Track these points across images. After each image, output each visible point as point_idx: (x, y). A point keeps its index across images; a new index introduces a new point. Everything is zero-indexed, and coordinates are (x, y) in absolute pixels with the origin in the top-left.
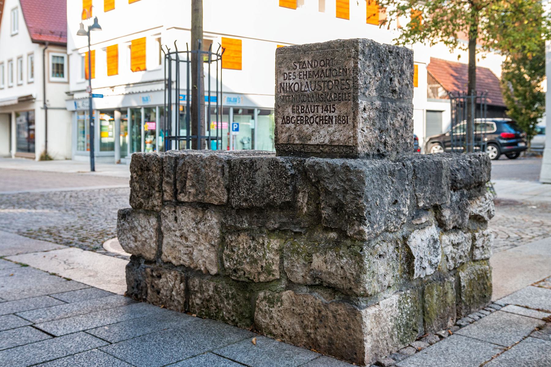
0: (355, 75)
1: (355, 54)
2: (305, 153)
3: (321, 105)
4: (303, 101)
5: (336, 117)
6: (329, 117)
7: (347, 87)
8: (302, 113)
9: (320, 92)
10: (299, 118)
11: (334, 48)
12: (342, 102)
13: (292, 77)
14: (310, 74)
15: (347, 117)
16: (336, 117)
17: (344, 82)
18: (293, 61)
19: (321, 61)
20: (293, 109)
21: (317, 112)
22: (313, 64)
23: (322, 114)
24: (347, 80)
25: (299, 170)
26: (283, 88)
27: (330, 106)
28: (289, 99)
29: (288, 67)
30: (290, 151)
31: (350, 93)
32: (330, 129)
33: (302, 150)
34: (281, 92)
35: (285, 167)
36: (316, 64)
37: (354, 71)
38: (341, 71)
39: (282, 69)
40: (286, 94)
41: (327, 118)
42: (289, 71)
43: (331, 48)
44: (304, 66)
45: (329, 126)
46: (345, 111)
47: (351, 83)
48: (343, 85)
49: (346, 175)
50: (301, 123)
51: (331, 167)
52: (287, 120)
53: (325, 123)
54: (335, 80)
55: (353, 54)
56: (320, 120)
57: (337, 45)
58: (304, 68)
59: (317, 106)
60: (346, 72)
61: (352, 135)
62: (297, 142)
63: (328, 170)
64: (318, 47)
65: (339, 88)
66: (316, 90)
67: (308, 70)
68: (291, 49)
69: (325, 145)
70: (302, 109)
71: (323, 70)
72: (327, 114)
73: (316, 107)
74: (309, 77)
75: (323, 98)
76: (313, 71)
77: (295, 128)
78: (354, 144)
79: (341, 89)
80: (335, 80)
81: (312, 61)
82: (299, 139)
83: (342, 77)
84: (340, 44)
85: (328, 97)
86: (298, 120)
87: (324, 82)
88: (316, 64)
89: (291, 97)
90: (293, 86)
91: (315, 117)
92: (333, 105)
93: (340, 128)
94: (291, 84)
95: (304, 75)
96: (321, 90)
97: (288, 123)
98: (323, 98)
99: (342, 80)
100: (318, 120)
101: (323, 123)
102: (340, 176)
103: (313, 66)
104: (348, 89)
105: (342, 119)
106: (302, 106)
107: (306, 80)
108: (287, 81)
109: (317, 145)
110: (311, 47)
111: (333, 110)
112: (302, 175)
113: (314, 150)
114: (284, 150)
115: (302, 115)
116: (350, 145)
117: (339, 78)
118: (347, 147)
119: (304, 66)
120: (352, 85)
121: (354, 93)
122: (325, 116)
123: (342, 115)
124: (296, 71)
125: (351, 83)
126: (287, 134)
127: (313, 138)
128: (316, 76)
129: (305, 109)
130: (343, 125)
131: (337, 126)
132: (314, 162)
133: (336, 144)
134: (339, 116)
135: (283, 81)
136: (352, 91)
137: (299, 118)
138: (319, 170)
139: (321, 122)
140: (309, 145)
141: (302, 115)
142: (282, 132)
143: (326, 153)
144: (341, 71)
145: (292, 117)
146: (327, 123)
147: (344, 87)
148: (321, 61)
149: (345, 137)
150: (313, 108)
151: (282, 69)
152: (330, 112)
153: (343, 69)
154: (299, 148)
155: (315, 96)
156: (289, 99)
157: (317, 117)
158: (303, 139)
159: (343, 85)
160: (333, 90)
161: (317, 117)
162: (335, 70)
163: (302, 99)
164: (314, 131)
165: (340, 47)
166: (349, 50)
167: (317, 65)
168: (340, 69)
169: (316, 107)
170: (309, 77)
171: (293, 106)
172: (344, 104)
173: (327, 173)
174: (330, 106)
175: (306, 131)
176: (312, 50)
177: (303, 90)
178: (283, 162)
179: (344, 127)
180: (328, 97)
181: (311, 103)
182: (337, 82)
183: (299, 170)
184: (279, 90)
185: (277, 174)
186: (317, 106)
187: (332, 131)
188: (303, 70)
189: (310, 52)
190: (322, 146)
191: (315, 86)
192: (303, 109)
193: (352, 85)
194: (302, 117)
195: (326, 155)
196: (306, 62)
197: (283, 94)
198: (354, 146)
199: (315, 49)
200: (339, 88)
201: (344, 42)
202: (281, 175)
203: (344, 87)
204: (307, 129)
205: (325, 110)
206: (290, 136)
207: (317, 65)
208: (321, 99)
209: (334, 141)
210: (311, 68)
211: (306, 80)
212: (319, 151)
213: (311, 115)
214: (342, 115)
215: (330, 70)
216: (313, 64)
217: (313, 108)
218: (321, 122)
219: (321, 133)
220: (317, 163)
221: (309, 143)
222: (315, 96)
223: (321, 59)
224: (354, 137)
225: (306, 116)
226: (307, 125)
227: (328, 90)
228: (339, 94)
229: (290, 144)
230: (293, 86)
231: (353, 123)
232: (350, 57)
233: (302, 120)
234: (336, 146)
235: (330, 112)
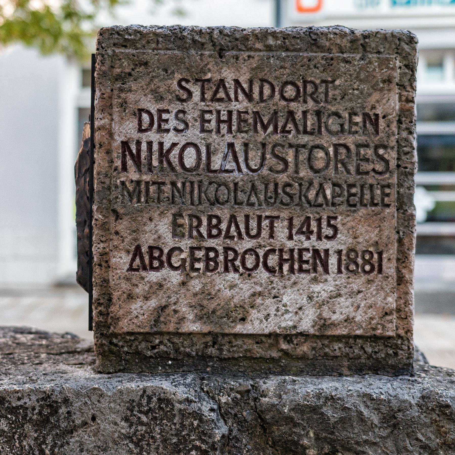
0: (404, 134)
1: (403, 75)
2: (221, 360)
3: (285, 214)
4: (217, 201)
5: (339, 252)
6: (316, 252)
7: (379, 167)
8: (210, 236)
9: (283, 178)
10: (200, 254)
11: (329, 50)
12: (363, 211)
13: (173, 123)
14: (239, 120)
15: (380, 254)
16: (339, 252)
17: (370, 152)
18: (178, 76)
19: (286, 83)
20: (175, 225)
21: (271, 236)
22: (256, 90)
23: (290, 244)
24: (376, 148)
25: (241, 422)
26: (137, 159)
27: (319, 221)
28: (160, 191)
29: (154, 91)
30: (165, 356)
31: (389, 186)
32: (317, 288)
33: (212, 351)
34: (125, 168)
35: (198, 416)
36: (267, 91)
37: (400, 122)
38: (358, 119)
39: (131, 97)
40: (146, 178)
41: (307, 256)
42: (161, 106)
43: (321, 48)
44: (221, 94)
45: (315, 280)
46: (373, 236)
47: (392, 156)
48: (367, 160)
49: (439, 433)
50: (207, 268)
51: (384, 409)
52: (152, 258)
53: (301, 270)
54: (336, 146)
55: (397, 74)
56: (281, 261)
57: (345, 43)
58: (221, 100)
59: (272, 219)
60: (376, 124)
61: (394, 306)
62: (195, 327)
63: (376, 419)
64: (271, 41)
65: (352, 169)
66: (265, 171)
67: (235, 106)
68: (165, 36)
69: (301, 334)
70: (210, 227)
71: (291, 114)
72: (306, 244)
73: (265, 223)
74: (240, 130)
75: (291, 196)
76: (256, 114)
77: (183, 284)
78: (401, 332)
79: (358, 172)
80: (336, 146)
81: (251, 82)
82: (199, 318)
83: (361, 138)
84: (352, 42)
85: (312, 194)
86: (195, 260)
87: (297, 148)
88: (267, 91)
89: (167, 188)
90: (176, 152)
91: (261, 253)
92: (329, 218)
93: (355, 287)
94: (167, 146)
95: (219, 121)
96: (285, 170)
97: (157, 269)
98: (291, 196)
99: (359, 146)
100: (273, 261)
101: (292, 270)
102: (420, 436)
103: (256, 95)
104: (380, 173)
105: (360, 261)
106: (210, 218)
107: (229, 138)
108: (153, 136)
109: (269, 336)
110: (246, 38)
111: (330, 232)
112: (252, 435)
113: (258, 351)
114: (138, 353)
115: (211, 243)
116: (390, 333)
117: (350, 140)
118: (375, 339)
119: (221, 94)
120: (393, 164)
121: (400, 185)
122: (301, 251)
123: (360, 248)
124: (188, 106)
125: (392, 156)
126: (153, 303)
127: (254, 314)
128: (265, 128)
129: (224, 226)
130: (364, 278)
131: (342, 279)
132: (318, 396)
133: (342, 331)
134: (351, 250)
135: (136, 135)
136: (394, 180)
137: (200, 254)
138: (342, 420)
139: (286, 267)
140: (236, 336)
141: (211, 243)
142: (131, 297)
143: (303, 358)
144: (358, 119)
145: (172, 250)
146: (307, 271)
147: (368, 167)
148: (286, 83)
149: (371, 312)
150: (253, 224)
151: (131, 97)
152: (319, 238)
153: (366, 116)
154: (199, 346)
155: (261, 187)
156: (160, 191)
157: (273, 251)
158: (214, 318)
159: (367, 160)
160: (331, 172)
161: (273, 251)
162: (337, 114)
163: (212, 195)
164: (260, 294)
165: (353, 50)
166: (384, 63)
167: (272, 96)
168: (353, 113)
169: (265, 223)
170: (240, 130)
171: (179, 215)
172: (368, 217)
173: (372, 426)
174: (319, 221)
175: (228, 293)
176: (251, 49)
177: (216, 165)
178: (188, 401)
179: (369, 282)
180: (312, 194)
181: (247, 210)
182: (343, 151)
183: (241, 422)
184: (118, 163)
185: (165, 440)
186: (272, 219)
187: (324, 295)
188: (217, 106)
189: (245, 55)
190: (288, 338)
191: (263, 158)
192: (217, 226)
193: (393, 164)
194: (209, 249)
195: (301, 364)
196: (230, 84)
197: (135, 176)
198: (399, 336)
199: (259, 45)
200: (352, 169)
201: (365, 37)
202: (185, 440)
203: (368, 167)
204: (232, 287)
205: (300, 232)
206: (163, 308)
207: (272, 96)
208: (286, 199)
209: (334, 325)
210: (246, 103)
211: (229, 138)
212: (275, 354)
213: (248, 244)
214: (360, 248)
215: (318, 113)
216: (256, 90)
217: (253, 224)
218: (286, 267)
219: (285, 299)
220: (331, 399)
221: (239, 328)
222: (261, 187)
223: (285, 78)
224: (399, 310)
225: (227, 249)
226: (232, 276)
227: (311, 174)
228: (353, 186)
229: (161, 334)
230: (176, 152)
231: (398, 271)
232: (389, 81)
233: (215, 260)
234: (338, 338)
235: (319, 238)
